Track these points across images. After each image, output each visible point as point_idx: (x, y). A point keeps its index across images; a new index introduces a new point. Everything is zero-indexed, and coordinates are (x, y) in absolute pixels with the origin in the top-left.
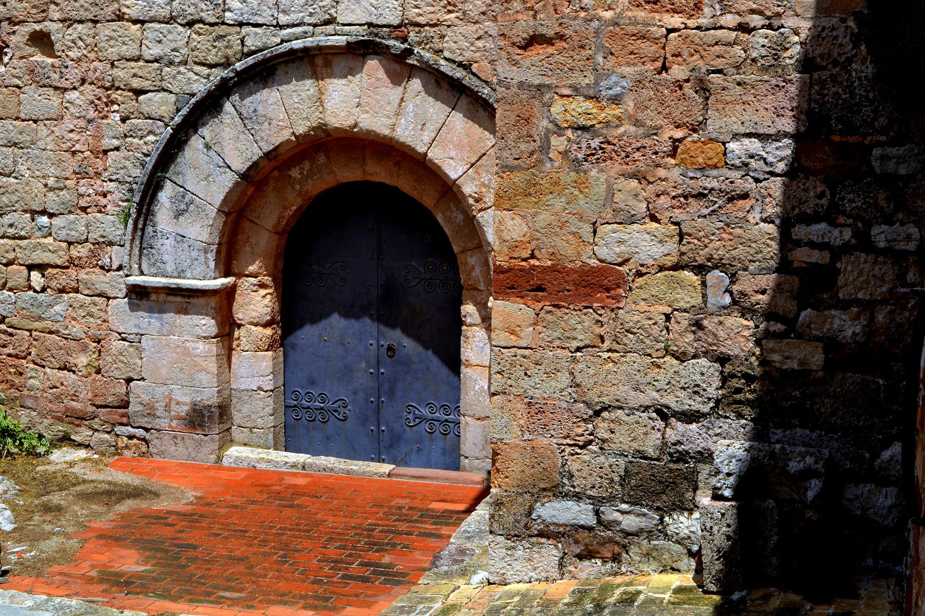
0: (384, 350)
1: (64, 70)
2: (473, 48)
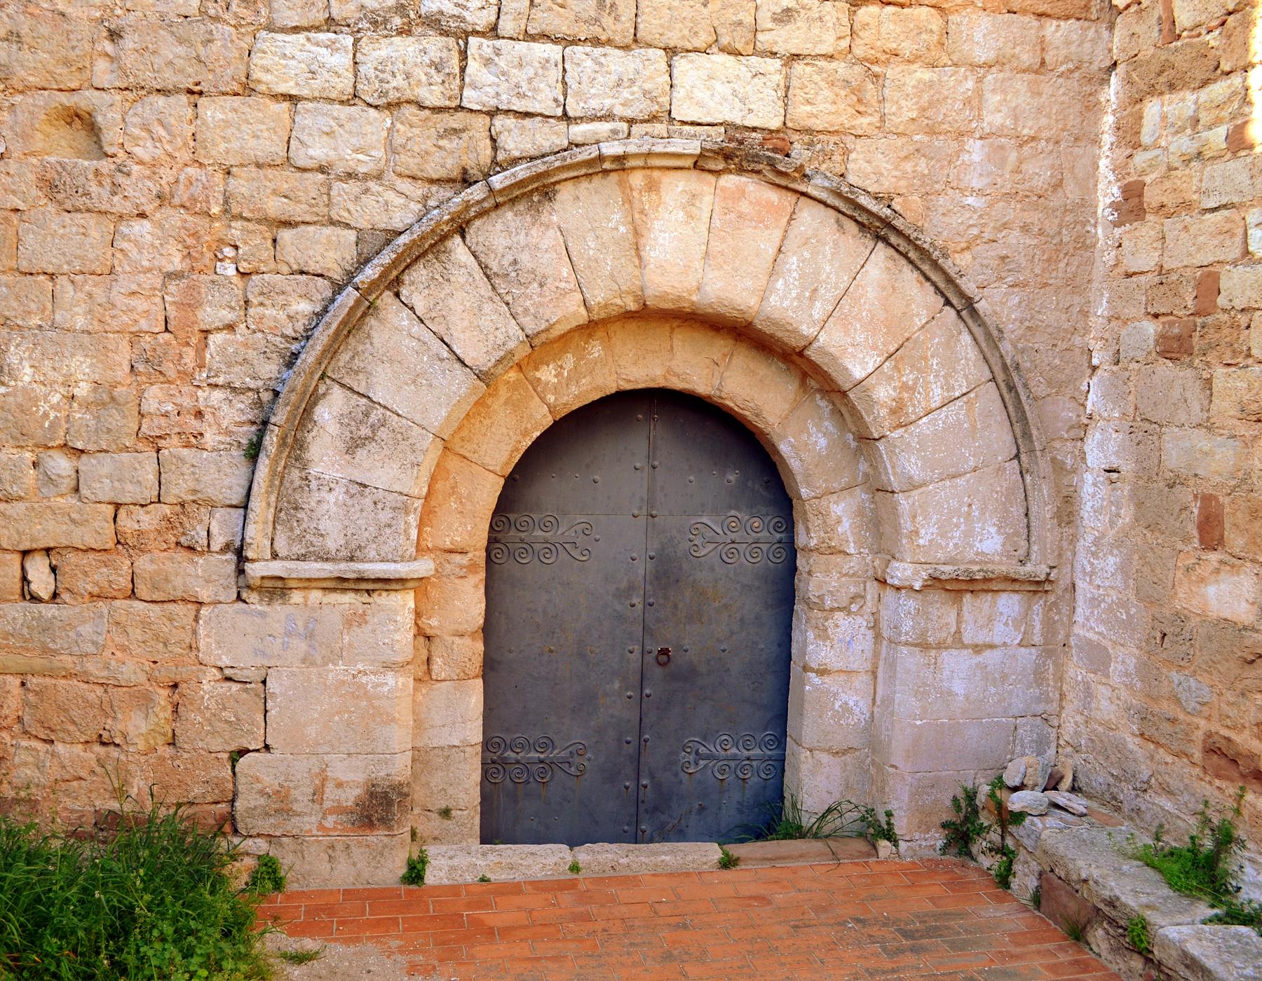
0: (650, 659)
1: (120, 179)
2: (897, 173)
